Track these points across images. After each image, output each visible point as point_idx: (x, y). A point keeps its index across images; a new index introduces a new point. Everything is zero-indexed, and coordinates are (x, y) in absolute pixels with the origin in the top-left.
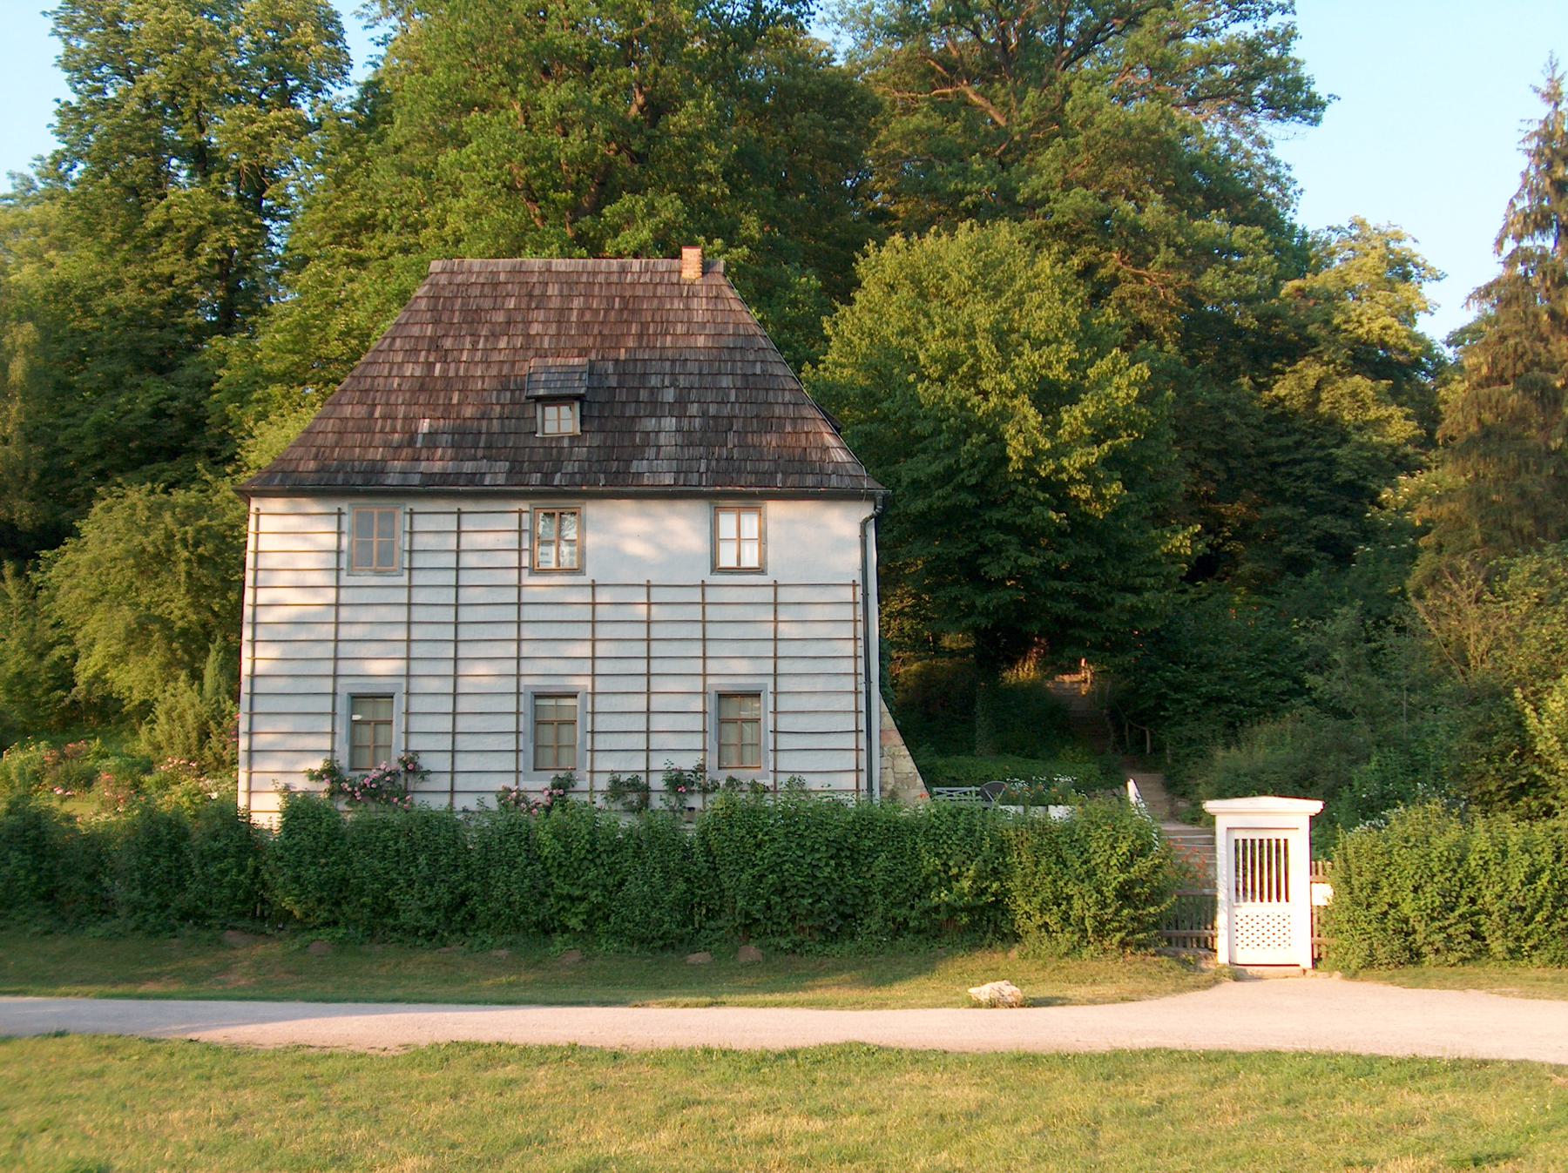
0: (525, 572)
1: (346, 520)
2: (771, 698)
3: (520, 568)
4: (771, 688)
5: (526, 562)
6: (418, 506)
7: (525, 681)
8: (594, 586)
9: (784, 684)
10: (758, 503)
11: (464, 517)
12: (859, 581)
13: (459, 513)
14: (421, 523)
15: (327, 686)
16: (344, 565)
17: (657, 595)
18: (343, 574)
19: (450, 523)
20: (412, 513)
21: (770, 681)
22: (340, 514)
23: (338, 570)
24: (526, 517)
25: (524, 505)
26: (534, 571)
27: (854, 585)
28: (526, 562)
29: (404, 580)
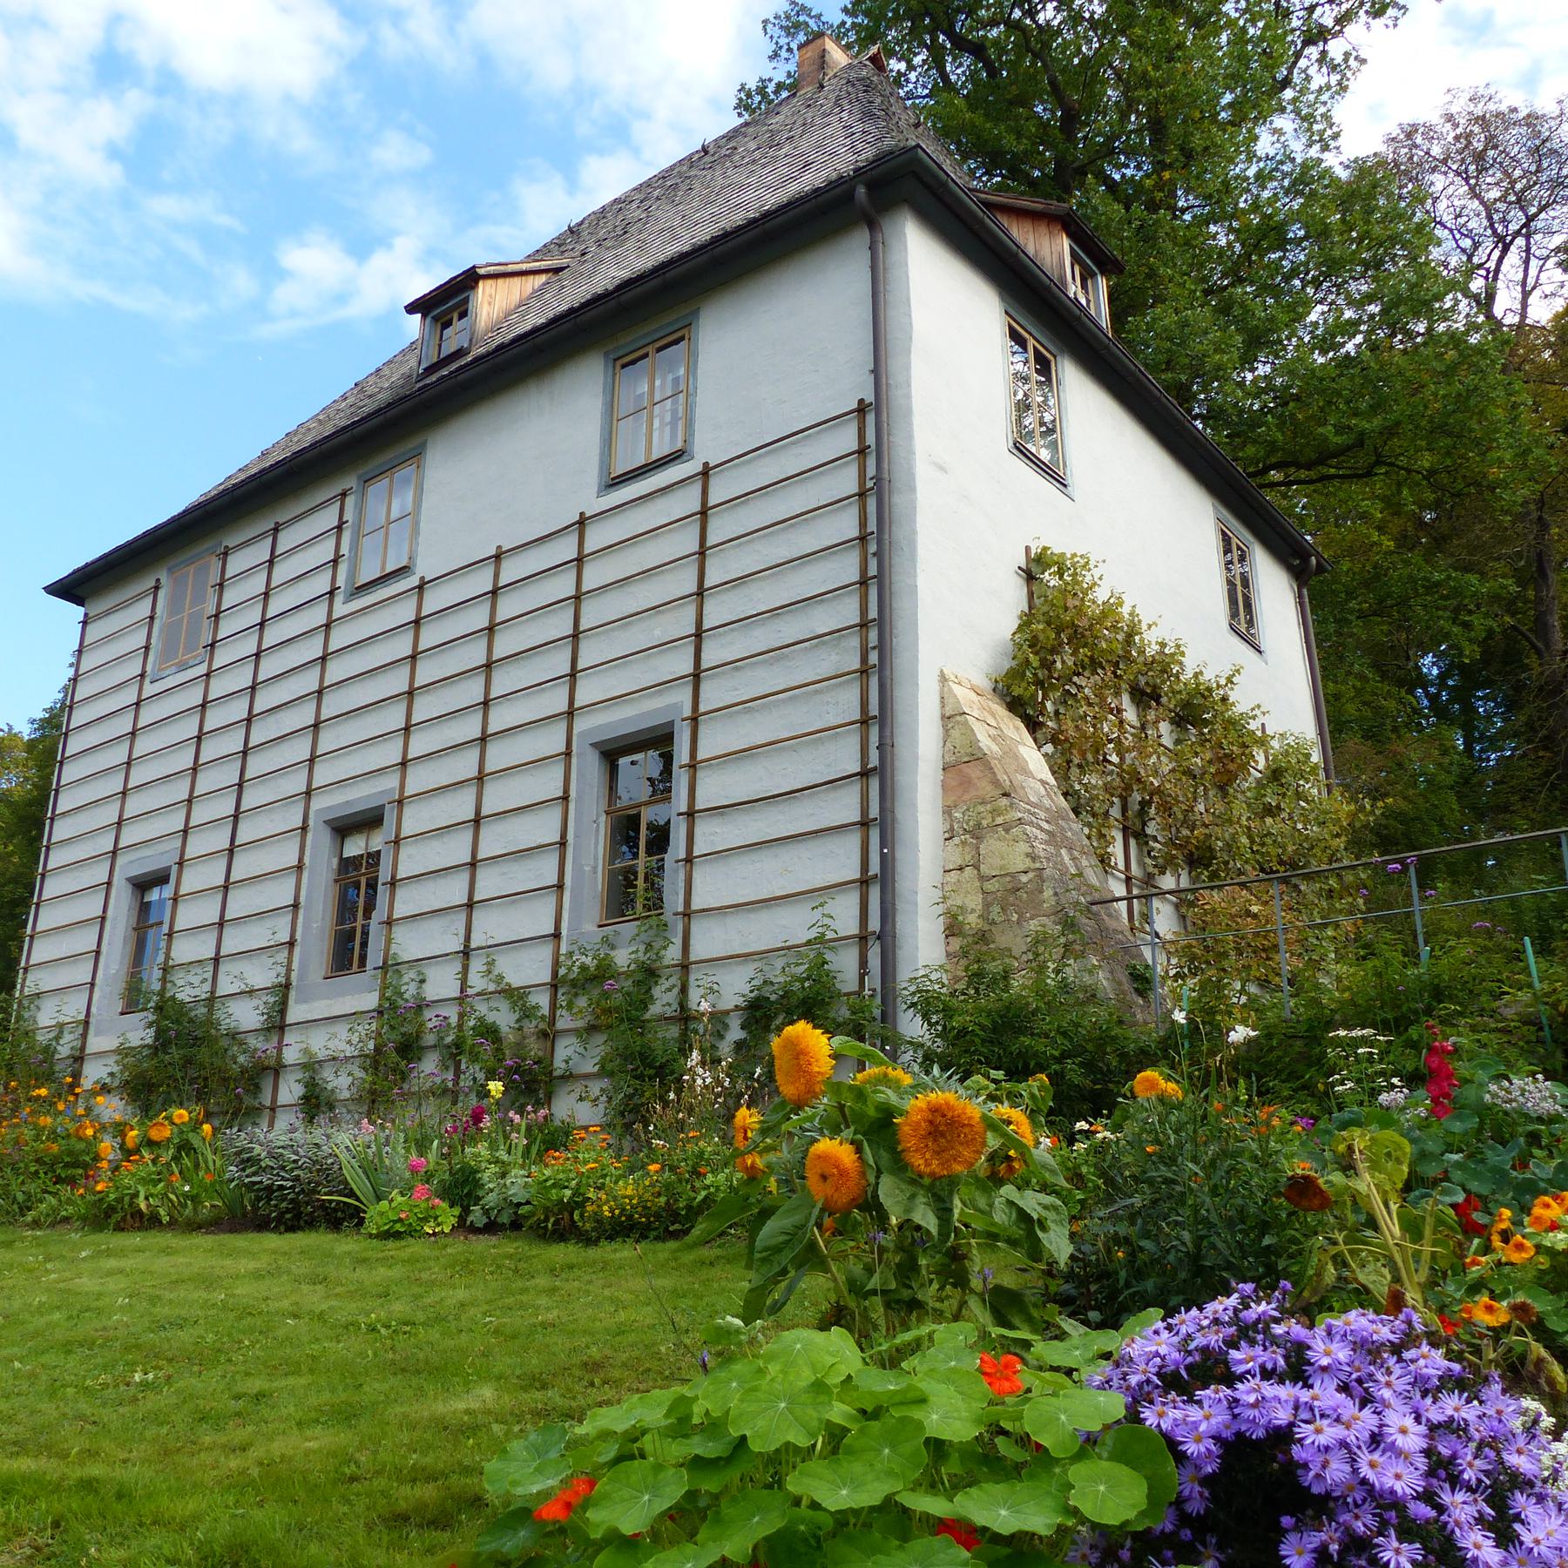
1: (161, 594)
3: (331, 593)
4: (687, 712)
8: (421, 587)
9: (713, 696)
11: (282, 536)
12: (870, 398)
13: (276, 530)
14: (236, 564)
16: (149, 668)
18: (147, 681)
19: (261, 552)
22: (157, 588)
23: (142, 675)
24: (350, 501)
25: (350, 482)
27: (862, 409)
28: (340, 582)
29: (203, 669)
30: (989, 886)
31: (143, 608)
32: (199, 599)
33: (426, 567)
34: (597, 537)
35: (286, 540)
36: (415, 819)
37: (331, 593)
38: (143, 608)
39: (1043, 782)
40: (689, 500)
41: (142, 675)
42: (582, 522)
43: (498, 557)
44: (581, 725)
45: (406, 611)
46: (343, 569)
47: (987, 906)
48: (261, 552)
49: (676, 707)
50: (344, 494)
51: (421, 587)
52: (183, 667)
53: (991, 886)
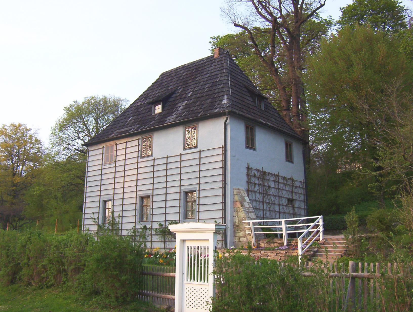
0: (139, 158)
1: (104, 149)
2: (198, 192)
4: (198, 189)
5: (139, 155)
6: (118, 142)
7: (138, 193)
8: (154, 159)
9: (202, 187)
10: (194, 124)
13: (126, 142)
14: (119, 147)
15: (98, 199)
17: (170, 160)
19: (124, 146)
20: (117, 144)
21: (198, 186)
22: (103, 148)
23: (102, 164)
24: (140, 140)
26: (142, 157)
27: (223, 147)
29: (114, 165)
30: (239, 219)
31: (101, 151)
32: (112, 151)
33: (155, 156)
34: (184, 158)
35: (129, 145)
36: (155, 199)
37: (138, 157)
38: (101, 151)
39: (248, 202)
40: (197, 155)
41: (102, 164)
42: (181, 155)
43: (167, 157)
44: (182, 188)
45: (151, 163)
46: (140, 152)
47: (239, 222)
48: (124, 146)
49: (196, 188)
50: (139, 139)
51: (154, 159)
52: (110, 164)
53: (239, 219)
